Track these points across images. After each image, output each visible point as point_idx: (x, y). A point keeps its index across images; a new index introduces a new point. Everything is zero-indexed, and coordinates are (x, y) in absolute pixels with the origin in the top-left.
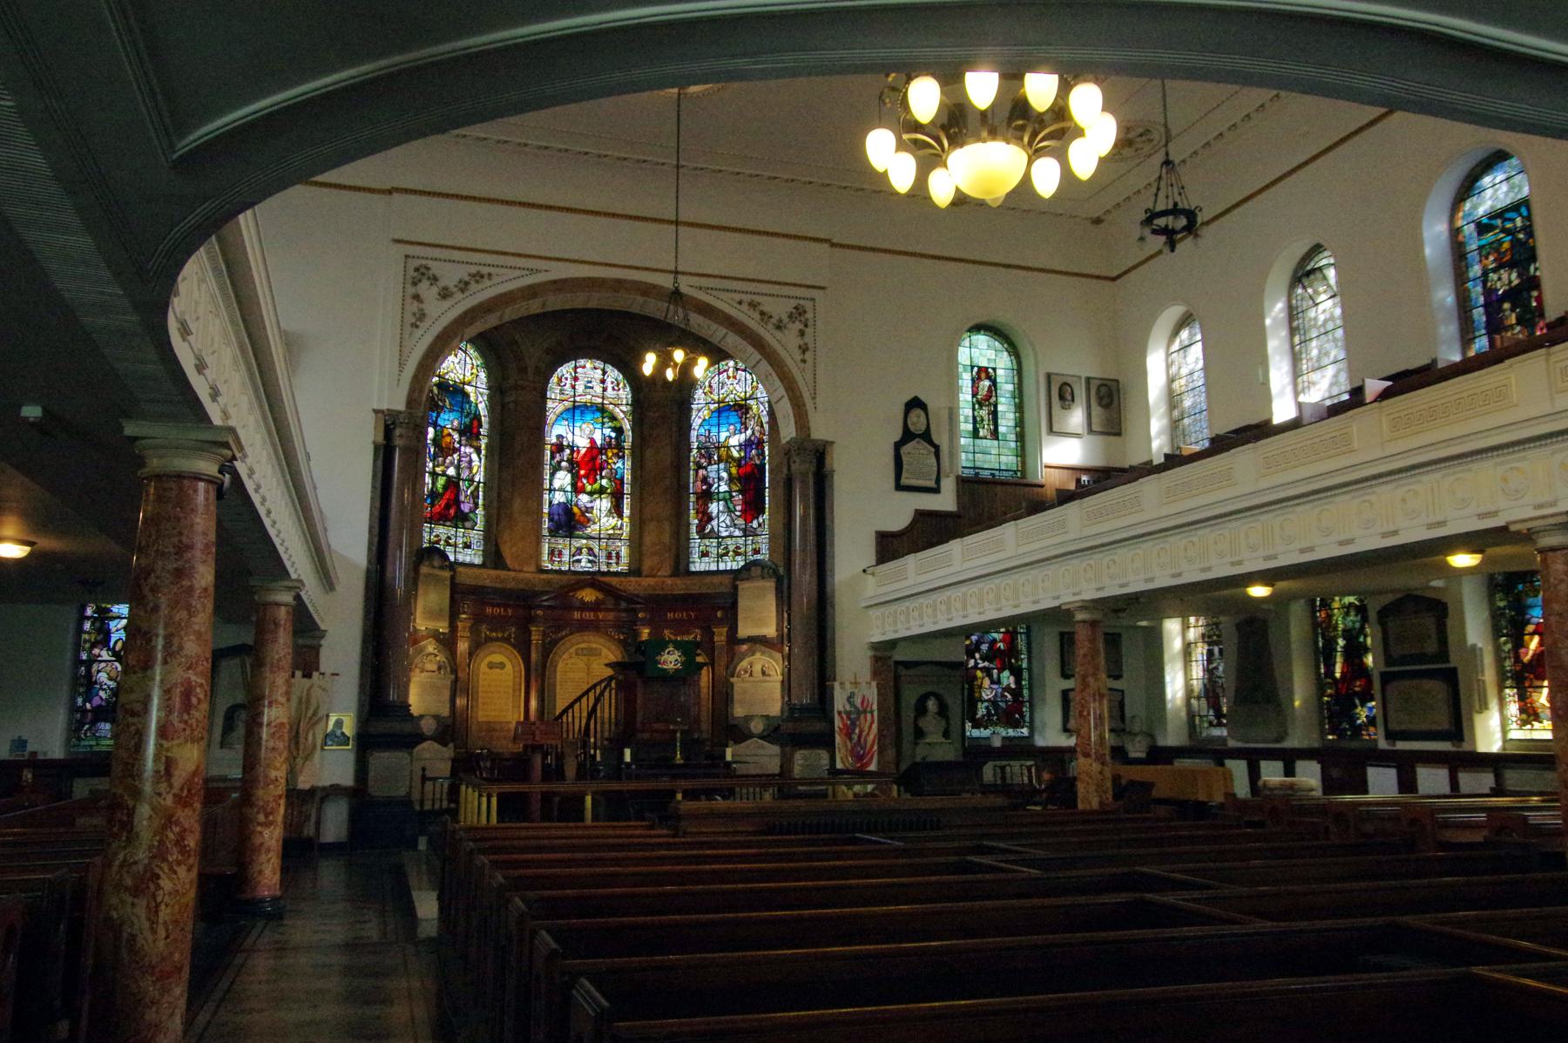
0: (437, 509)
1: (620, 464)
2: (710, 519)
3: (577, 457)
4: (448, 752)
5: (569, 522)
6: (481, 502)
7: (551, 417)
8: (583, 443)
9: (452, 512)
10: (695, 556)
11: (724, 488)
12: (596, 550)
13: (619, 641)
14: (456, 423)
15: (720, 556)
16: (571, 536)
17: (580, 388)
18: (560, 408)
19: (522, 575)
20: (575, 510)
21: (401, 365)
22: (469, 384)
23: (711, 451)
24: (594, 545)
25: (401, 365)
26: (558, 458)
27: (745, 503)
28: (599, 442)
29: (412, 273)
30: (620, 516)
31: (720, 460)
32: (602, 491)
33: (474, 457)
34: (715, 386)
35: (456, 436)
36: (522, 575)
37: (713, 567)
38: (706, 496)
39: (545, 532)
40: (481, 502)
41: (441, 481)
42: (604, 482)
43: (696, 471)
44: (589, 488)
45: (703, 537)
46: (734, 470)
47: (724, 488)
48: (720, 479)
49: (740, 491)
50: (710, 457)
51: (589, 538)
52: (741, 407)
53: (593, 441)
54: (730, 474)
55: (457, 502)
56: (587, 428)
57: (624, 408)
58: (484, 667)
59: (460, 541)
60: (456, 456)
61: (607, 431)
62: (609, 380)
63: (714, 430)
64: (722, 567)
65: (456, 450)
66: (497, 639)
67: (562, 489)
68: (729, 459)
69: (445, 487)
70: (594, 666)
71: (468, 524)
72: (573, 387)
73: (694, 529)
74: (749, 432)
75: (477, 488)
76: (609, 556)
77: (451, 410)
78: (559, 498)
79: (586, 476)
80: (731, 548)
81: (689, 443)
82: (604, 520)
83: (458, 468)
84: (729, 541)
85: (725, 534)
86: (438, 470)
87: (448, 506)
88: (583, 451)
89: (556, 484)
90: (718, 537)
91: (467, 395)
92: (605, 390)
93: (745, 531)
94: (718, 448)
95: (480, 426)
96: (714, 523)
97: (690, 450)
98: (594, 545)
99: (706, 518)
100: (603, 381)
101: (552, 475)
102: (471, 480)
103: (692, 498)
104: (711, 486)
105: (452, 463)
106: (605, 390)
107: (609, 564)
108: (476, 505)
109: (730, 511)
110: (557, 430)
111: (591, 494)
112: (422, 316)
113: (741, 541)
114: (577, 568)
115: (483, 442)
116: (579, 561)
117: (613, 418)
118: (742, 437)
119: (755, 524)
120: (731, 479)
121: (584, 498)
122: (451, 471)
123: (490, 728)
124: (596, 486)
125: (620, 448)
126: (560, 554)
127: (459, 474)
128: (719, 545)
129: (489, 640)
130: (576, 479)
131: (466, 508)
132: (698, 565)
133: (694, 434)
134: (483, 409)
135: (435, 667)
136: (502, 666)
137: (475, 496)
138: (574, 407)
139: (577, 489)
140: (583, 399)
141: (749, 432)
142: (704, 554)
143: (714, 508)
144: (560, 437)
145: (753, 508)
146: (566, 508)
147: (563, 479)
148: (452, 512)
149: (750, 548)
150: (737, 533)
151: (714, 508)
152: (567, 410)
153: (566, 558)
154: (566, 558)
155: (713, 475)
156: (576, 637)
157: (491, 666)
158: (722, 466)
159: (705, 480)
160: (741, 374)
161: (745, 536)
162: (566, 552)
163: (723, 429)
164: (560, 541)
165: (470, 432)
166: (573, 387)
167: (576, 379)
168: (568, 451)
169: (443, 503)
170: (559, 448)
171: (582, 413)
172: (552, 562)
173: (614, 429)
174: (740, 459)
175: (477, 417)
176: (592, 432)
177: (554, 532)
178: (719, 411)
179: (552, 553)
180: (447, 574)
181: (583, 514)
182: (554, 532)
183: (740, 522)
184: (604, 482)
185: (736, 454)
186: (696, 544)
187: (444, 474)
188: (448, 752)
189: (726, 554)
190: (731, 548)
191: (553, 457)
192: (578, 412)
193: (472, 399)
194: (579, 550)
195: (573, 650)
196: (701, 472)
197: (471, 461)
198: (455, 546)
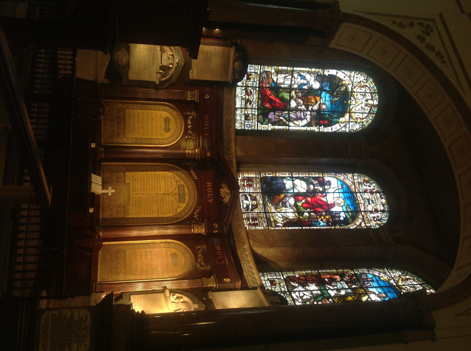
0: (269, 92)
1: (322, 223)
3: (319, 196)
4: (102, 78)
5: (273, 192)
6: (277, 127)
7: (341, 177)
8: (330, 199)
9: (268, 105)
11: (332, 293)
12: (256, 210)
13: (193, 214)
14: (324, 107)
16: (262, 193)
17: (367, 196)
18: (349, 183)
19: (233, 144)
20: (283, 196)
21: (368, 13)
22: (350, 117)
24: (260, 209)
25: (368, 13)
26: (315, 182)
28: (333, 210)
29: (426, 23)
30: (285, 225)
32: (300, 213)
33: (305, 122)
35: (316, 107)
36: (233, 144)
39: (263, 175)
40: (277, 127)
41: (286, 96)
42: (306, 214)
44: (299, 204)
51: (265, 205)
53: (333, 205)
55: (274, 109)
56: (341, 201)
57: (363, 225)
58: (165, 114)
59: (249, 112)
60: (303, 107)
61: (343, 216)
62: (379, 214)
65: (307, 107)
66: (186, 125)
67: (294, 186)
69: (282, 99)
70: (171, 198)
71: (261, 117)
72: (365, 191)
75: (285, 124)
76: (254, 219)
77: (331, 102)
78: (288, 184)
79: (307, 202)
82: (279, 215)
83: (296, 109)
86: (293, 93)
87: (271, 101)
88: (324, 199)
89: (297, 182)
91: (343, 116)
92: (371, 212)
95: (325, 126)
97: (352, 269)
98: (260, 209)
100: (376, 211)
101: (302, 179)
102: (290, 120)
105: (298, 104)
106: (371, 212)
107: (248, 219)
108: (274, 124)
110: (334, 181)
111: (296, 205)
112: (401, 25)
114: (242, 198)
115: (315, 129)
116: (247, 199)
117: (354, 218)
121: (292, 201)
122: (293, 104)
123: (121, 120)
124: (302, 209)
125: (334, 223)
126: (250, 186)
127: (292, 110)
129: (186, 118)
130: (304, 195)
131: (271, 116)
134: (335, 128)
135: (165, 63)
136: (167, 130)
137: (279, 123)
138: (352, 193)
139: (297, 196)
140: (360, 198)
144: (329, 183)
146: (282, 189)
147: (301, 187)
148: (268, 105)
152: (348, 187)
153: (247, 190)
154: (247, 190)
156: (191, 184)
157: (167, 120)
162: (251, 190)
164: (259, 186)
165: (320, 118)
166: (365, 191)
167: (371, 193)
168: (321, 189)
169: (273, 97)
170: (322, 183)
171: (349, 198)
172: (243, 180)
173: (345, 218)
175: (330, 124)
176: (339, 205)
177: (264, 181)
179: (249, 179)
180: (229, 79)
181: (281, 200)
182: (264, 181)
184: (306, 214)
187: (291, 98)
188: (102, 78)
191: (315, 178)
192: (349, 195)
193: (342, 119)
194: (254, 199)
195: (182, 183)
196: (338, 277)
197: (302, 119)
198: (246, 108)
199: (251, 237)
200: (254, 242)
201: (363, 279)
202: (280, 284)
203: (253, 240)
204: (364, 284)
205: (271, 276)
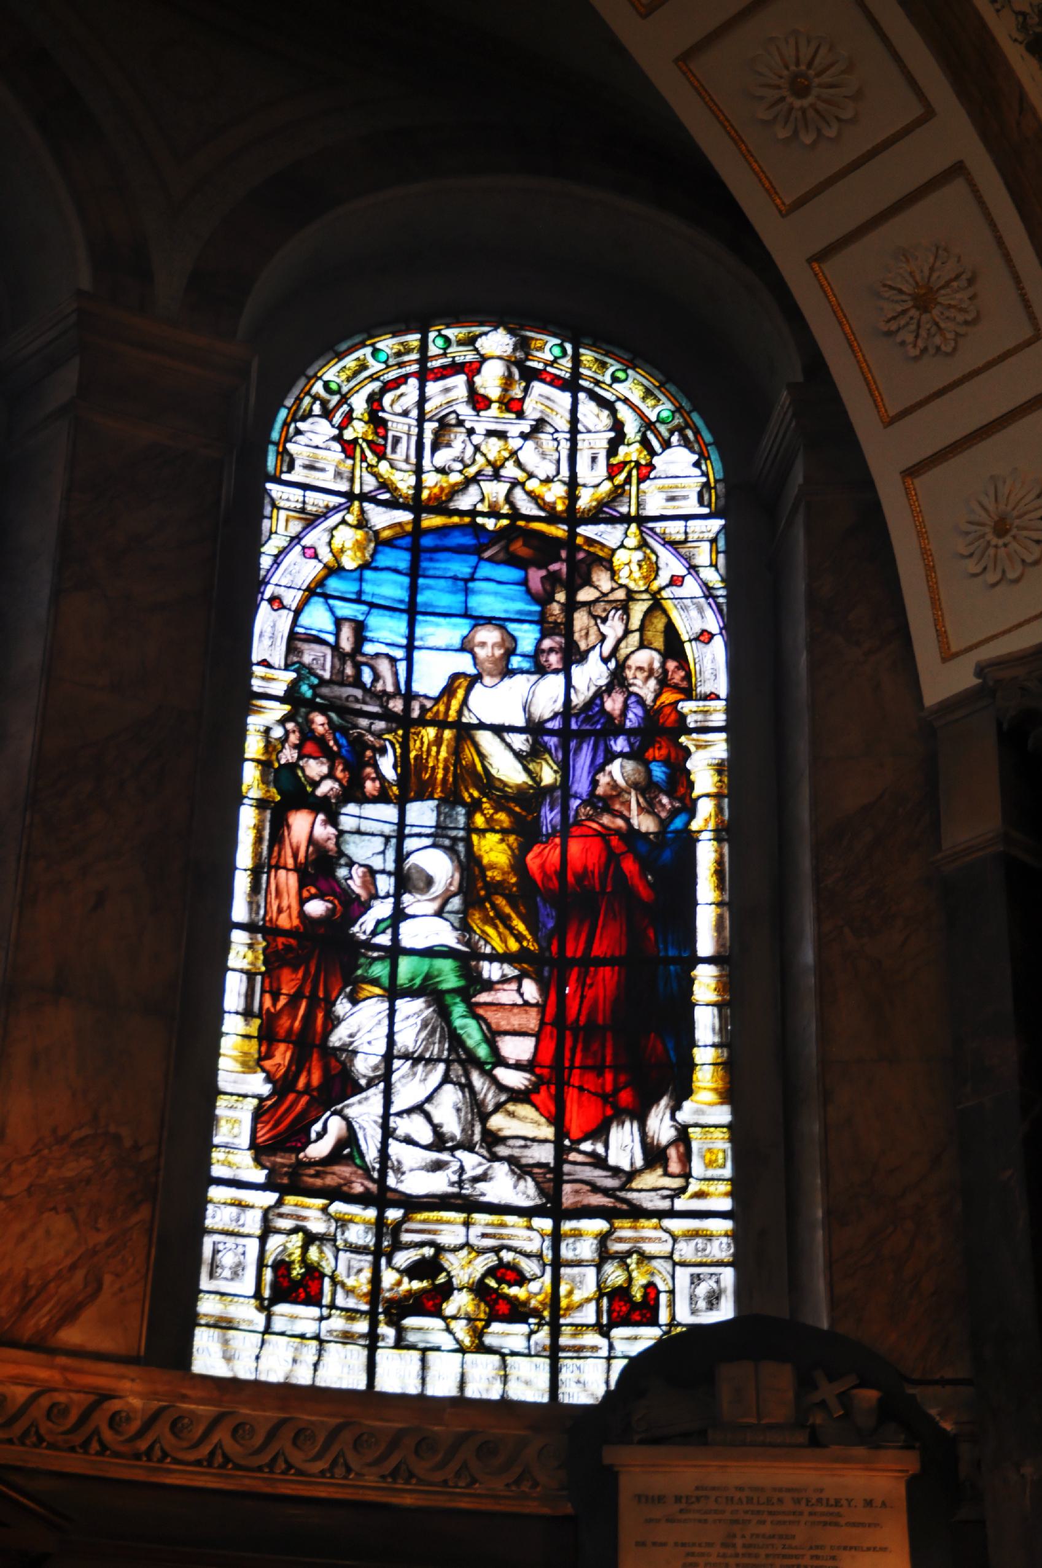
2: (341, 1084)
10: (229, 1282)
15: (389, 1312)
23: (357, 727)
27: (554, 1023)
31: (411, 785)
34: (399, 426)
37: (343, 1370)
38: (323, 957)
43: (277, 817)
45: (289, 1180)
46: (494, 851)
47: (427, 929)
48: (406, 880)
49: (525, 963)
50: (354, 760)
52: (544, 550)
54: (470, 866)
63: (387, 630)
64: (397, 1374)
68: (464, 786)
73: (234, 1126)
74: (590, 675)
80: (464, 1269)
81: (240, 662)
84: (450, 1230)
85: (417, 1183)
90: (380, 1197)
93: (550, 1180)
94: (405, 723)
96: (365, 1110)
97: (247, 700)
99: (313, 1077)
103: (241, 952)
104: (355, 907)
109: (459, 1061)
113: (528, 1237)
118: (548, 696)
119: (623, 1145)
120: (474, 888)
128: (385, 1243)
132: (241, 1344)
133: (269, 631)
141: (590, 675)
142: (294, 1284)
143: (361, 1026)
145: (612, 1056)
149: (582, 1285)
150: (503, 1187)
151: (361, 1026)
155: (364, 850)
158: (422, 814)
159: (321, 868)
160: (543, 399)
161: (552, 1207)
163: (439, 633)
174: (531, 798)
178: (417, 548)
183: (524, 1124)
185: (508, 770)
186: (238, 1220)
189: (430, 1303)
190: (464, 1269)
196: (300, 824)
199: (39, 1319)
200: (89, 1314)
201: (338, 679)
202: (310, 1239)
203: (69, 1314)
204: (383, 697)
205: (237, 1272)
